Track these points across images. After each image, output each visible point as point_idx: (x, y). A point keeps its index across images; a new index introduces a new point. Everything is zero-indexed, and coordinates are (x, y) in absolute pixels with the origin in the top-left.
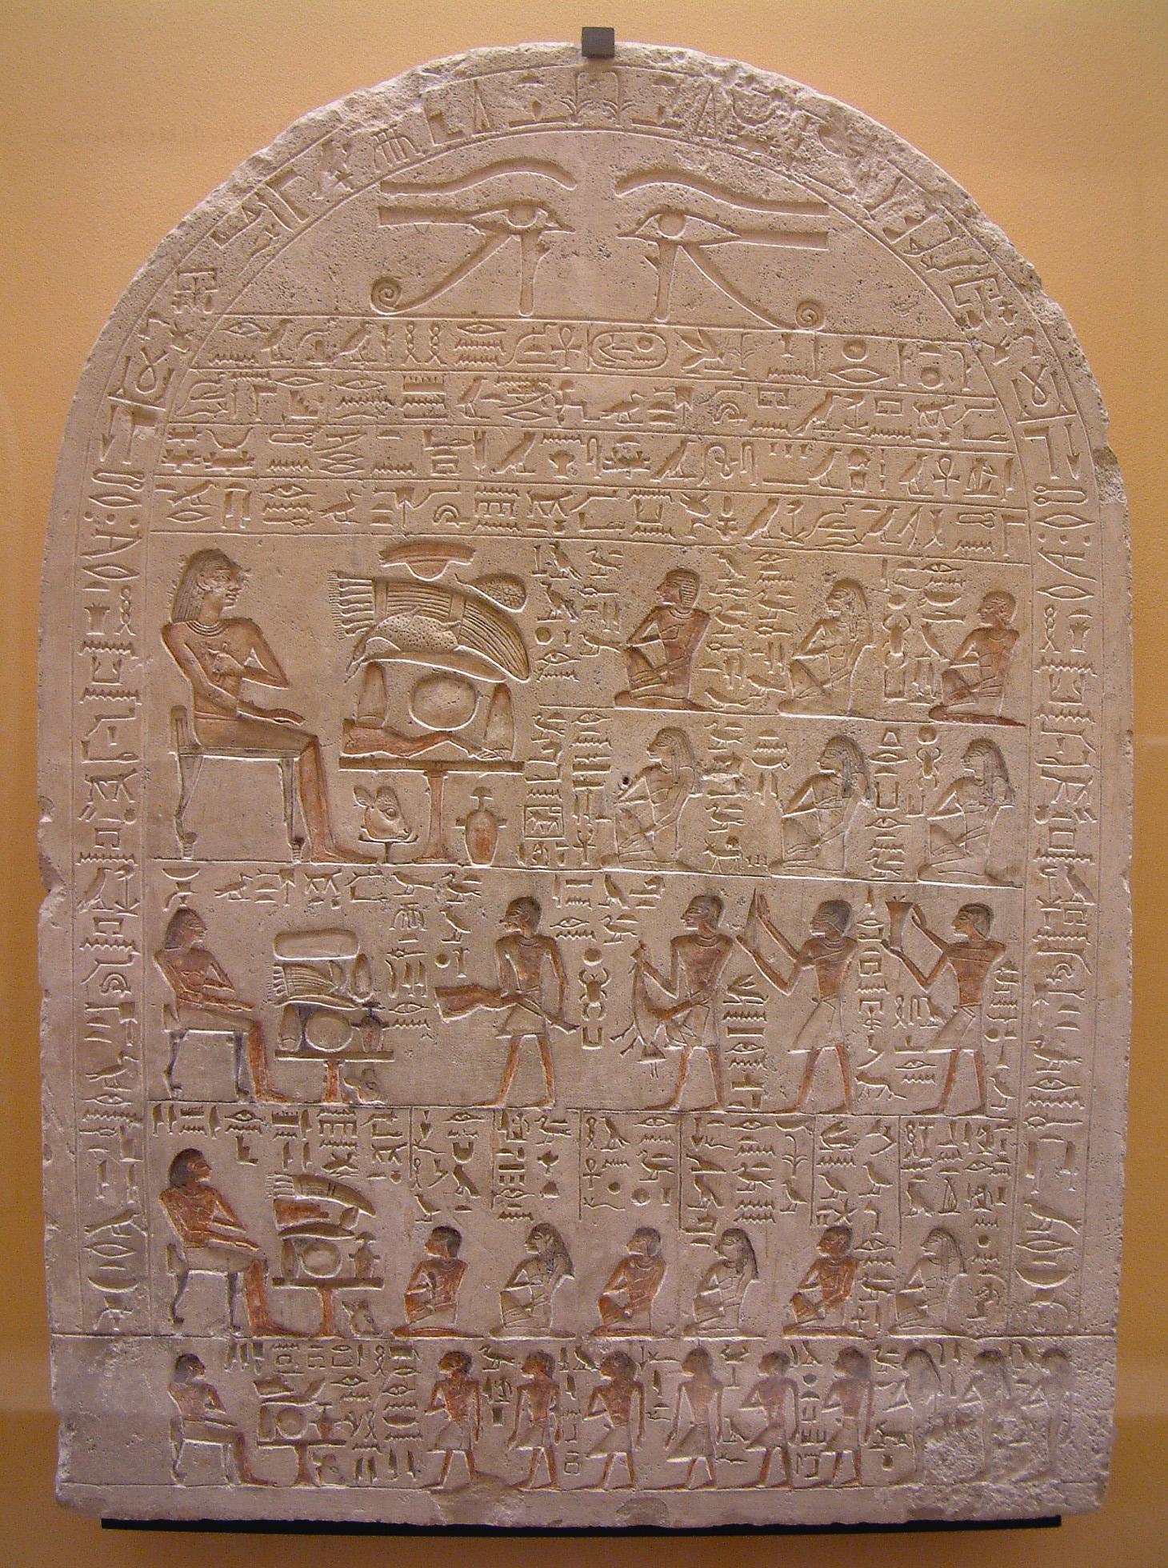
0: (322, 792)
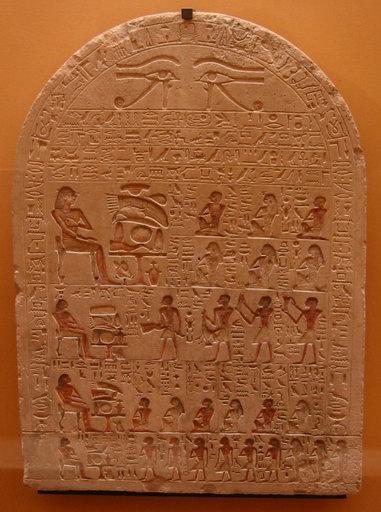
0: (104, 263)
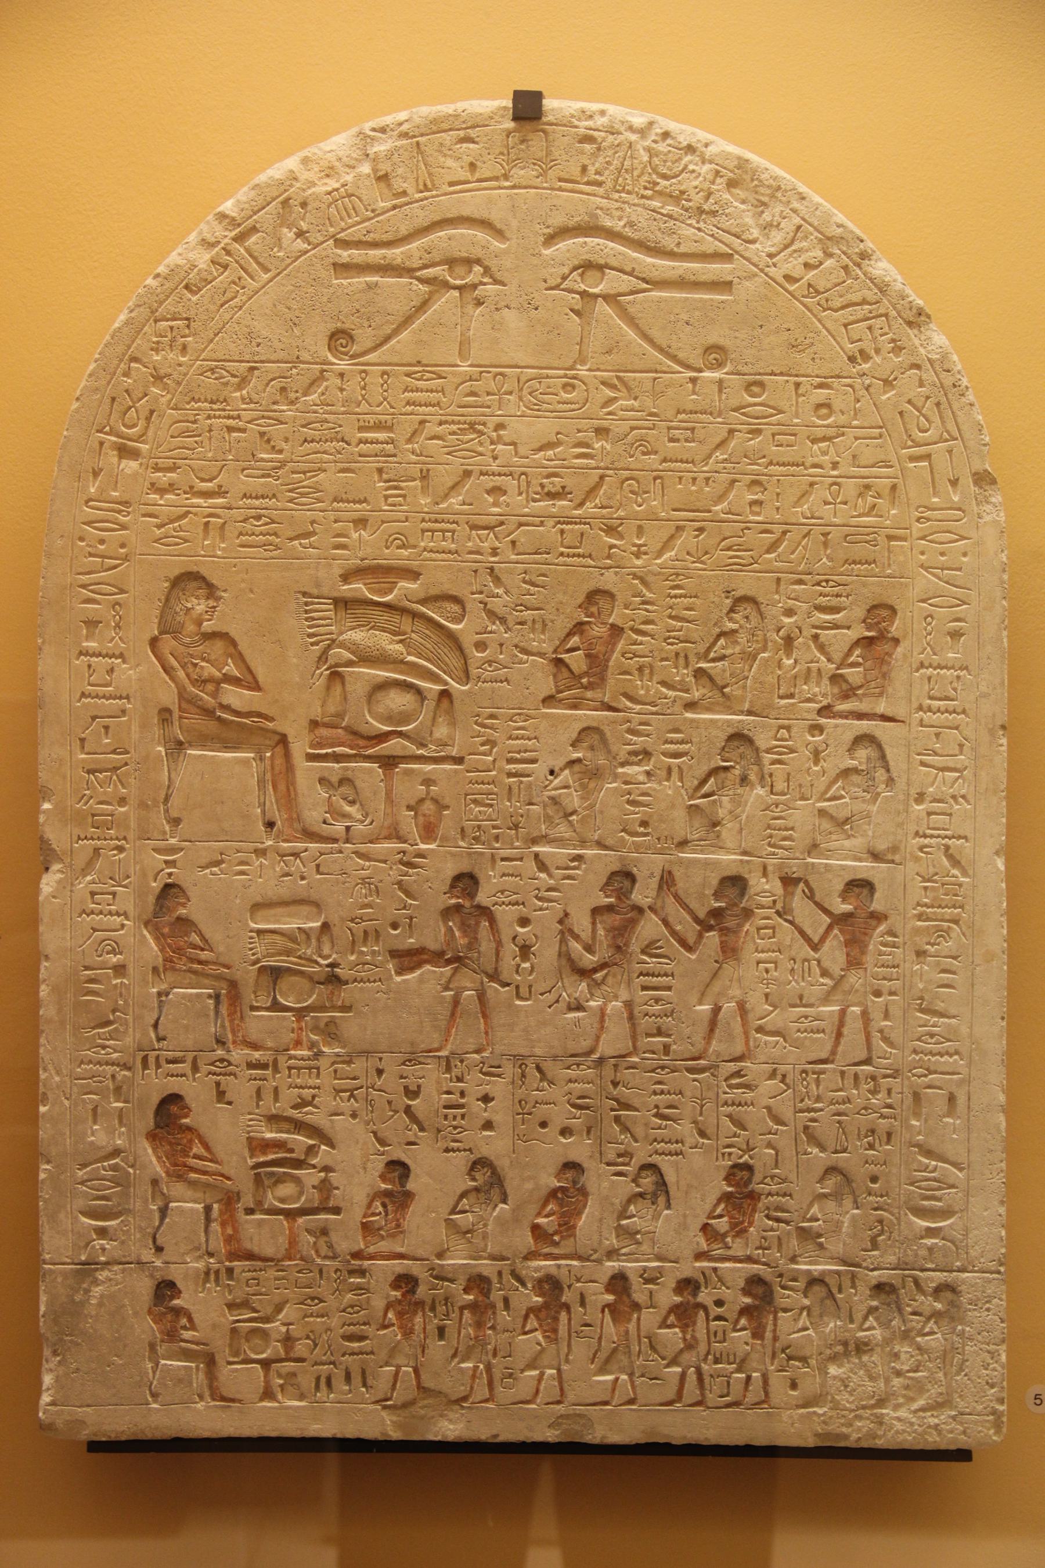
0: (291, 783)
